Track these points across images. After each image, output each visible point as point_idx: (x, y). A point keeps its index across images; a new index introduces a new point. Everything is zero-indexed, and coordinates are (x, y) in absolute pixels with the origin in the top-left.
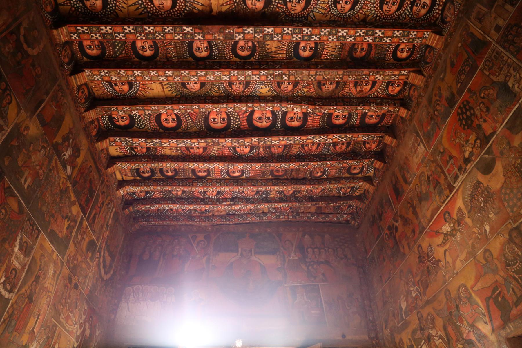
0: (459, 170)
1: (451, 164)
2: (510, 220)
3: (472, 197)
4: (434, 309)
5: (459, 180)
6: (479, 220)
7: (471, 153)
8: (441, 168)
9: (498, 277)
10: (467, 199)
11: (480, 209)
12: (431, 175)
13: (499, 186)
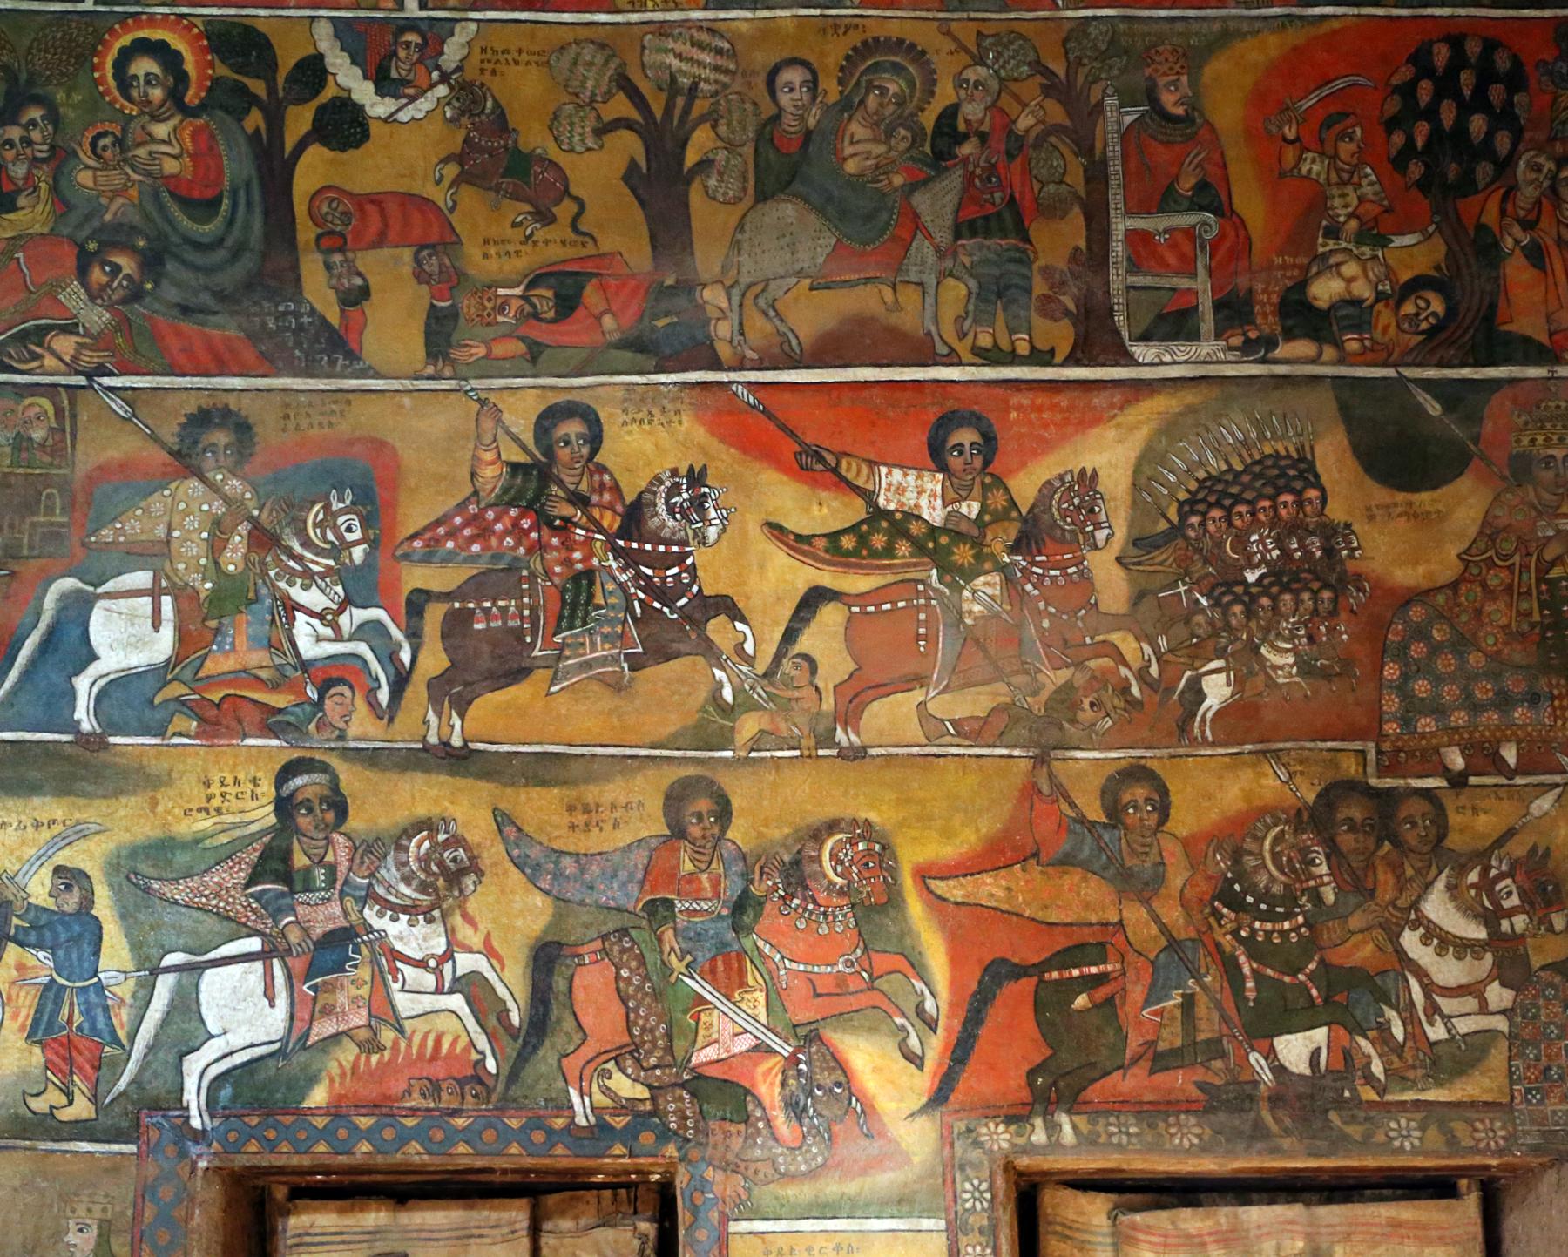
0: (1218, 306)
1: (1189, 233)
2: (1371, 746)
3: (1212, 494)
4: (502, 820)
5: (1183, 350)
6: (1187, 621)
7: (1353, 314)
8: (1097, 175)
9: (1135, 914)
10: (1175, 481)
11: (1229, 585)
12: (983, 137)
13: (1406, 576)
